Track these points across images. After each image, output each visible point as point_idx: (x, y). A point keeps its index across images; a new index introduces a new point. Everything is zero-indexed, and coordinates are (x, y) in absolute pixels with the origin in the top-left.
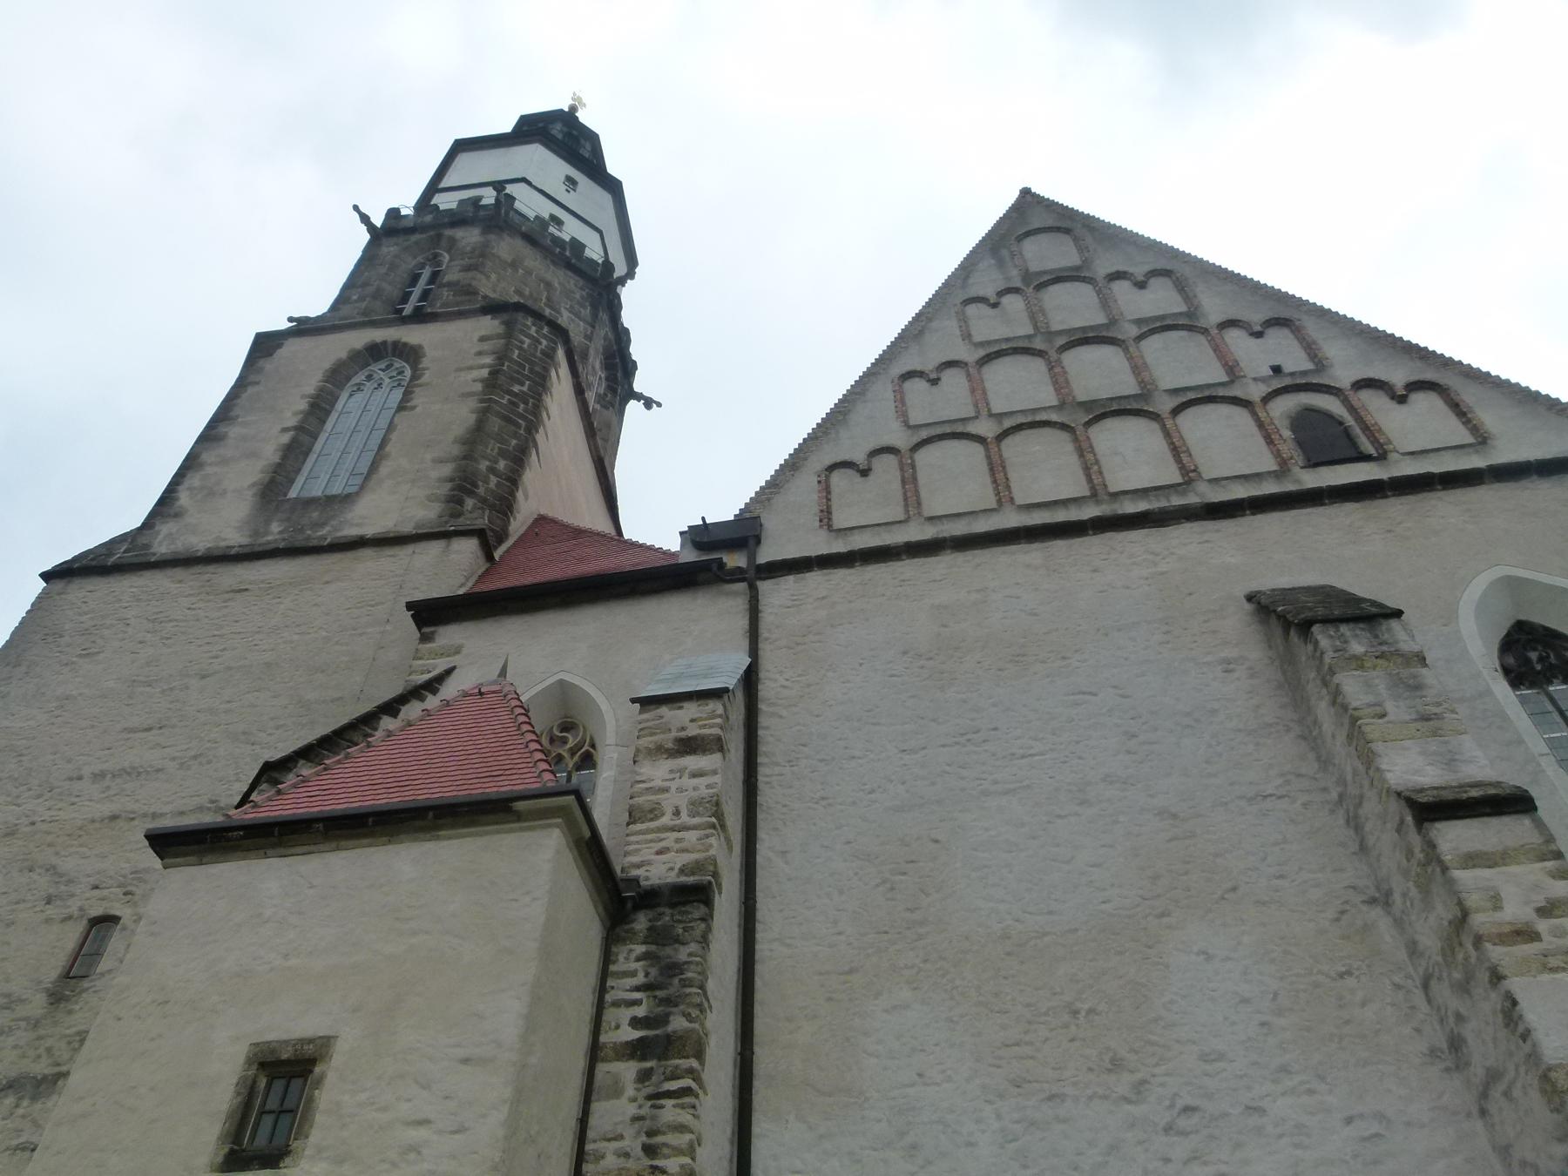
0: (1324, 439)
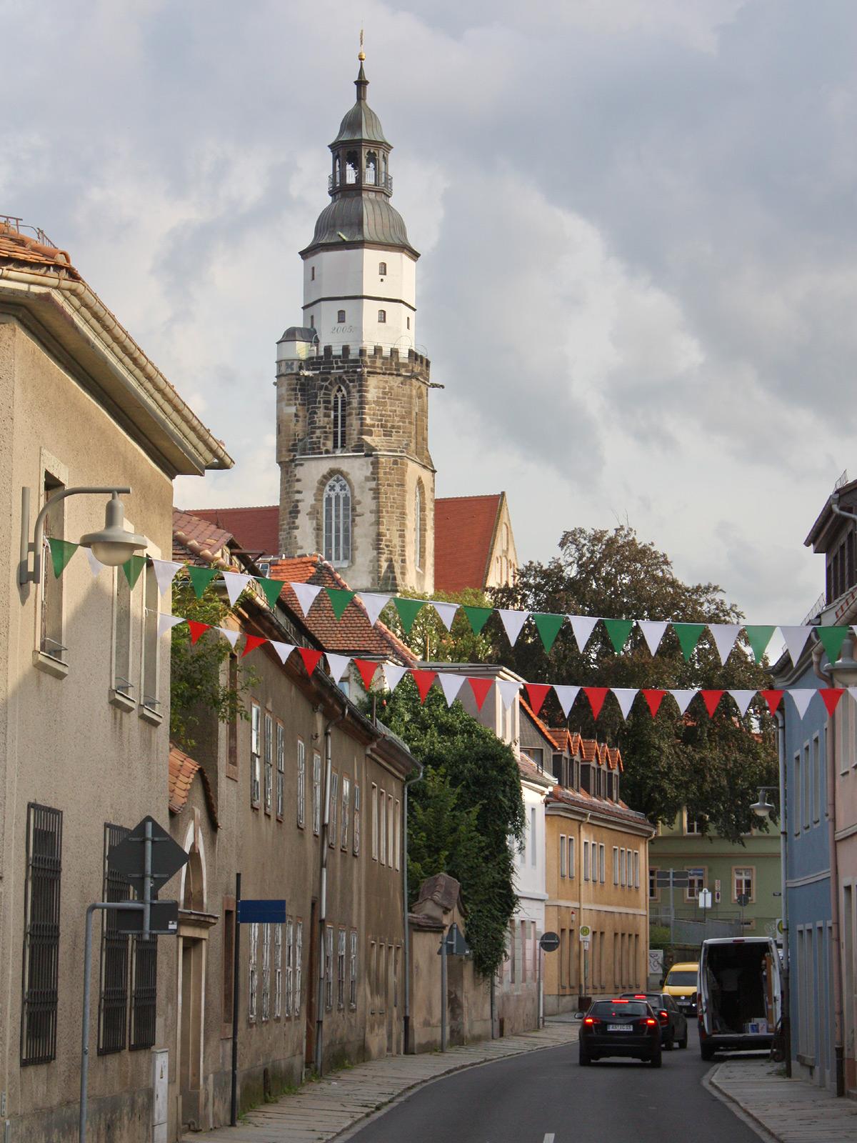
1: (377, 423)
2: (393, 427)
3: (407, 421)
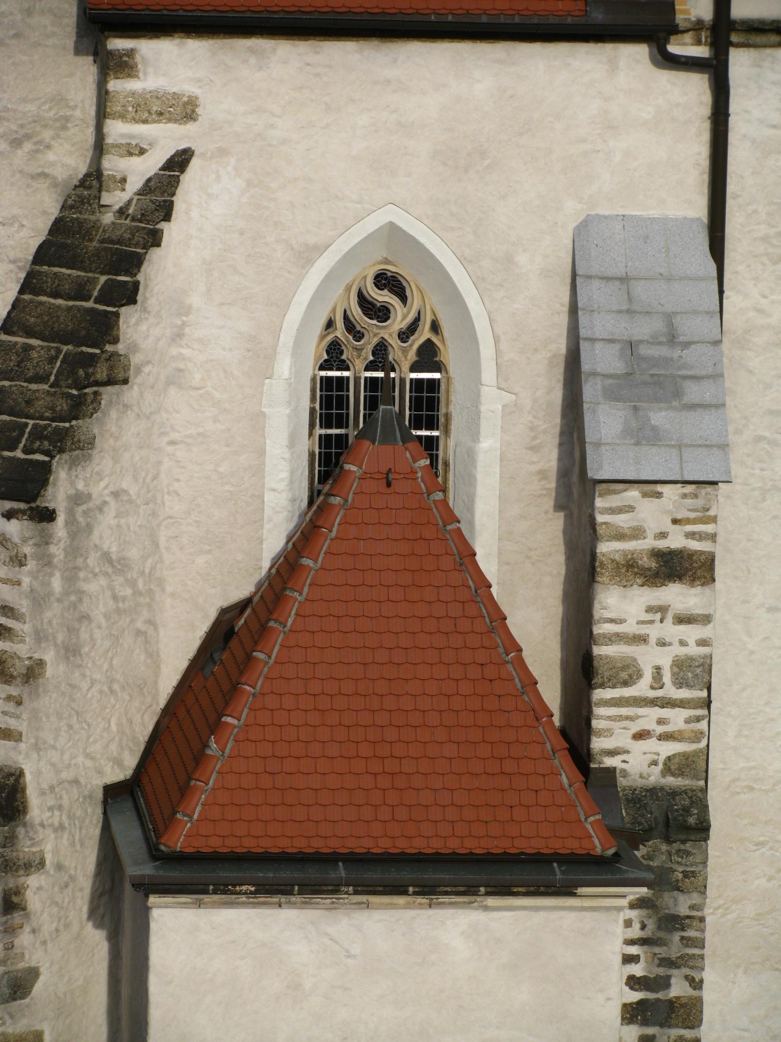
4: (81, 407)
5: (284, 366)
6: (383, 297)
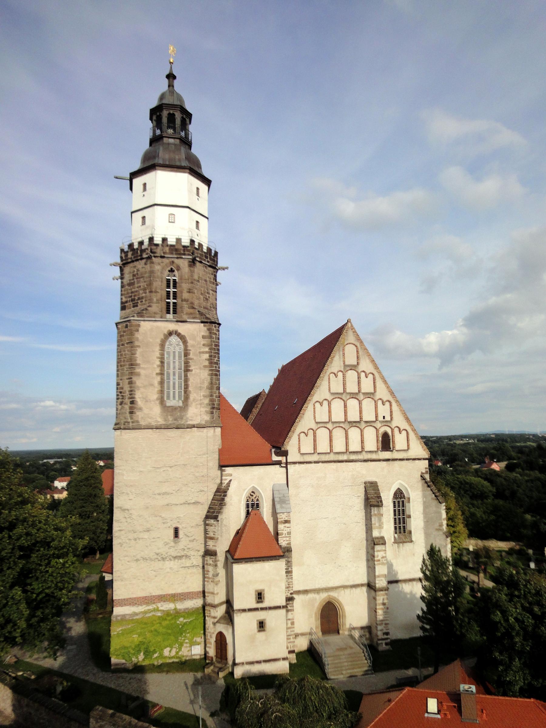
0: (386, 443)
1: (129, 299)
2: (139, 299)
3: (147, 291)
4: (221, 509)
5: (243, 502)
6: (252, 494)
